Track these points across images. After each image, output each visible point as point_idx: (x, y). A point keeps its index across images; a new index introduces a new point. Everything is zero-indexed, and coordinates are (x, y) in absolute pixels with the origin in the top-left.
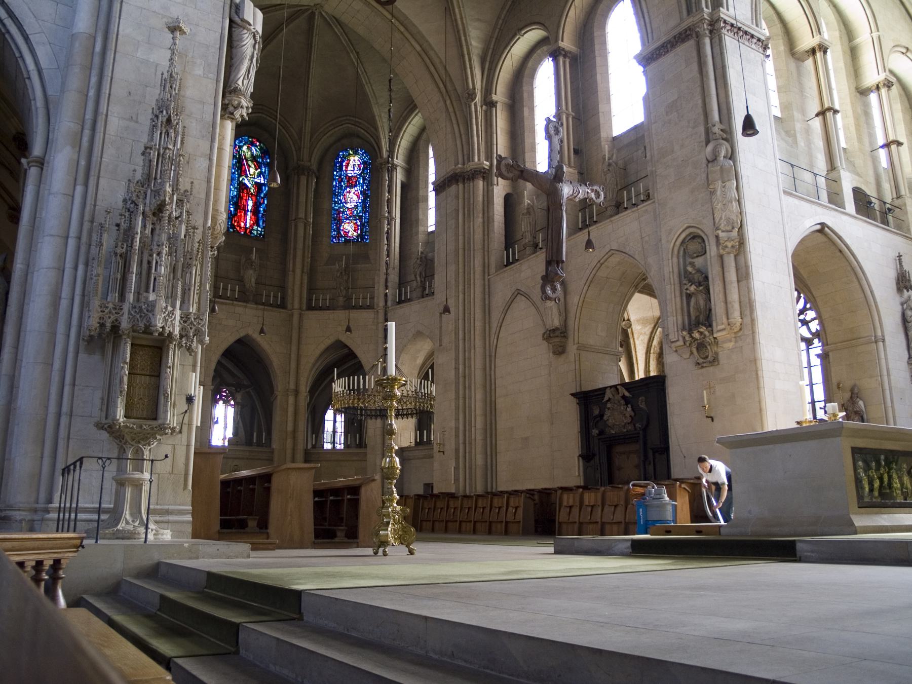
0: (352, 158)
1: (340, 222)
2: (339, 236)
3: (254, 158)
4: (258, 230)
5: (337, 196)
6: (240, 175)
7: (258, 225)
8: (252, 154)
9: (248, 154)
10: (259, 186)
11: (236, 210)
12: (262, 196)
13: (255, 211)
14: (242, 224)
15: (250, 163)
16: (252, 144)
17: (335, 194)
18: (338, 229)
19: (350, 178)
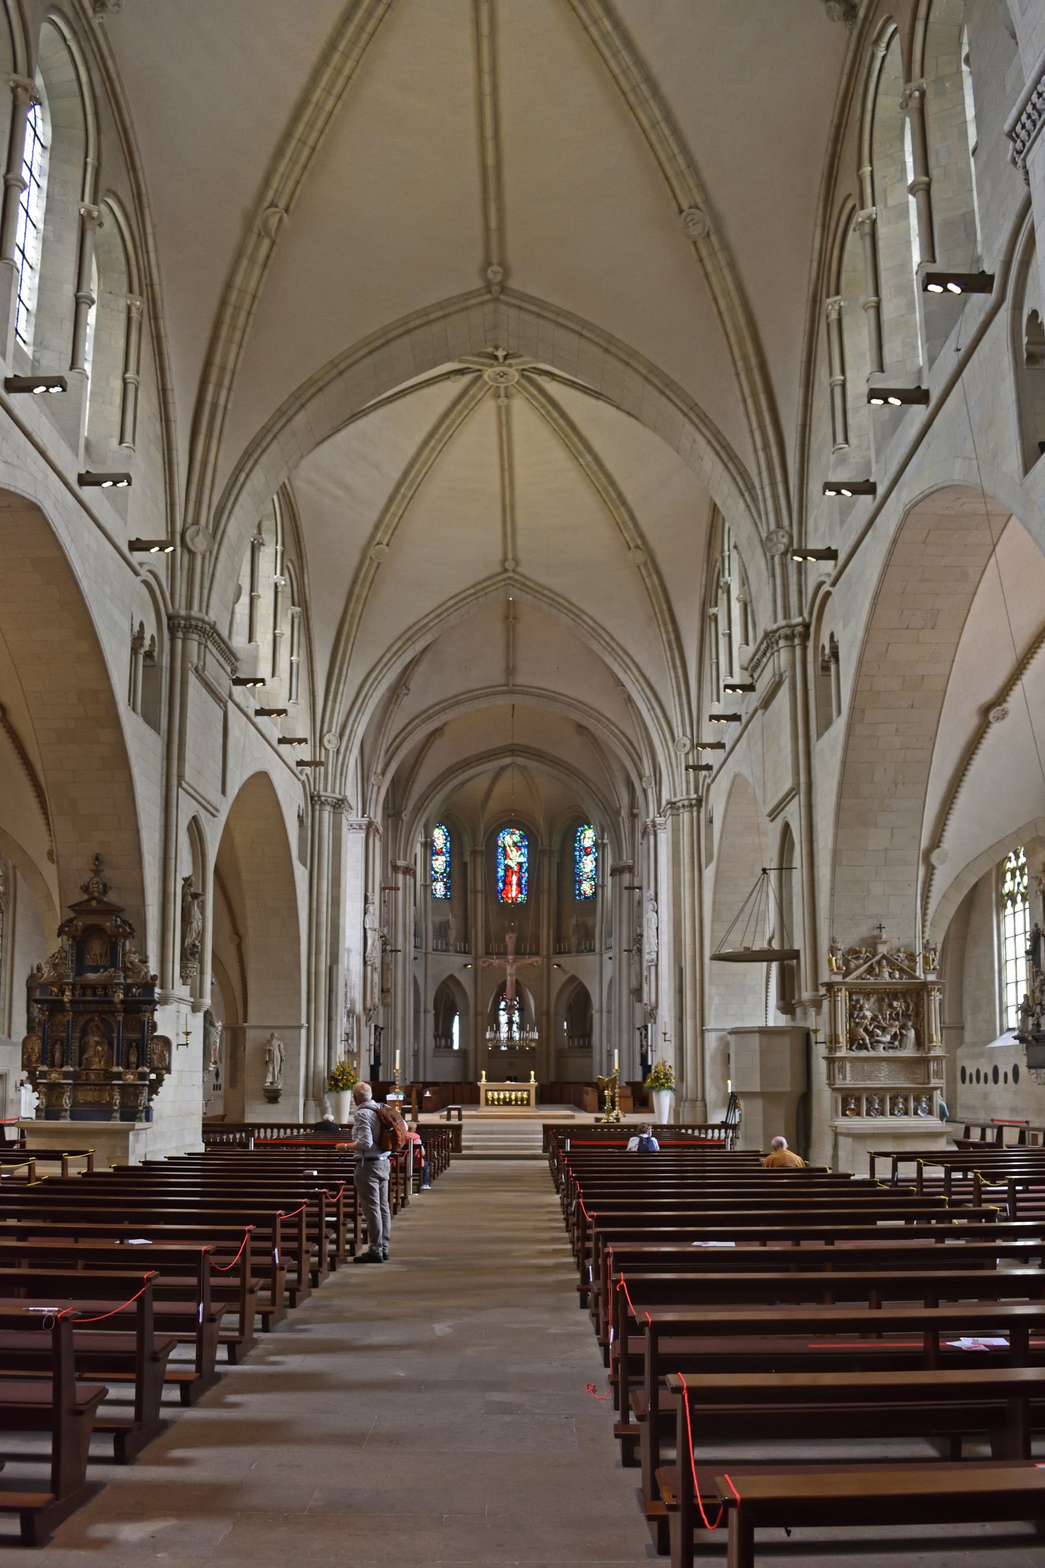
0: (586, 832)
1: (580, 882)
2: (580, 894)
3: (515, 844)
4: (521, 898)
5: (578, 863)
6: (505, 859)
7: (522, 894)
8: (514, 842)
9: (511, 843)
10: (520, 864)
11: (504, 886)
12: (523, 871)
13: (519, 884)
14: (510, 895)
15: (512, 848)
16: (513, 833)
17: (575, 862)
18: (579, 890)
19: (586, 849)
